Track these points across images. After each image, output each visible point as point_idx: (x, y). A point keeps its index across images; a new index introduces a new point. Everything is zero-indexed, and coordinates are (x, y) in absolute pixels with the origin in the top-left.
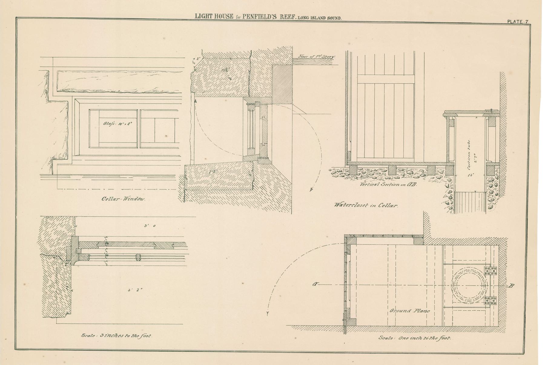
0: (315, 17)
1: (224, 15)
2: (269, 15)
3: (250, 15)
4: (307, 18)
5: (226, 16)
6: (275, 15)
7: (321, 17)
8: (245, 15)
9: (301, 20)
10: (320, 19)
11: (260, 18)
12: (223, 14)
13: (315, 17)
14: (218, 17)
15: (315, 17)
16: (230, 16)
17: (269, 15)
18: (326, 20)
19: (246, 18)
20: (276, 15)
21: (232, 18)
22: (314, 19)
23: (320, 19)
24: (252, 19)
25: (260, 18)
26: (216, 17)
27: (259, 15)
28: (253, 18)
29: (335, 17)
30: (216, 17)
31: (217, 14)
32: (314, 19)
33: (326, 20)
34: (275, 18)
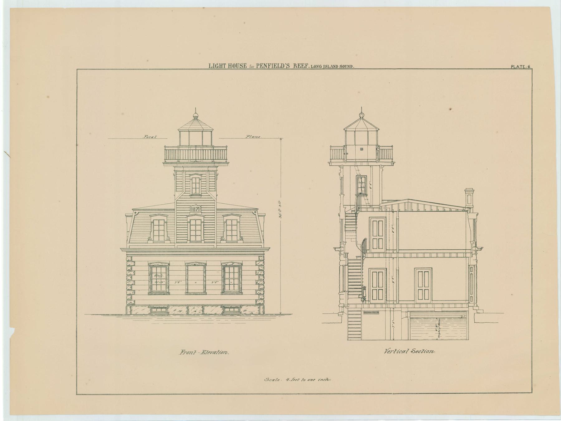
1: (238, 64)
2: (283, 65)
3: (264, 64)
5: (240, 66)
6: (288, 64)
7: (334, 66)
8: (258, 65)
9: (314, 68)
12: (237, 64)
16: (243, 66)
17: (283, 65)
18: (339, 68)
19: (259, 67)
21: (245, 67)
22: (326, 67)
25: (273, 67)
26: (230, 67)
28: (266, 66)
30: (230, 67)
31: (231, 64)
32: (326, 67)
33: (339, 68)
34: (288, 67)
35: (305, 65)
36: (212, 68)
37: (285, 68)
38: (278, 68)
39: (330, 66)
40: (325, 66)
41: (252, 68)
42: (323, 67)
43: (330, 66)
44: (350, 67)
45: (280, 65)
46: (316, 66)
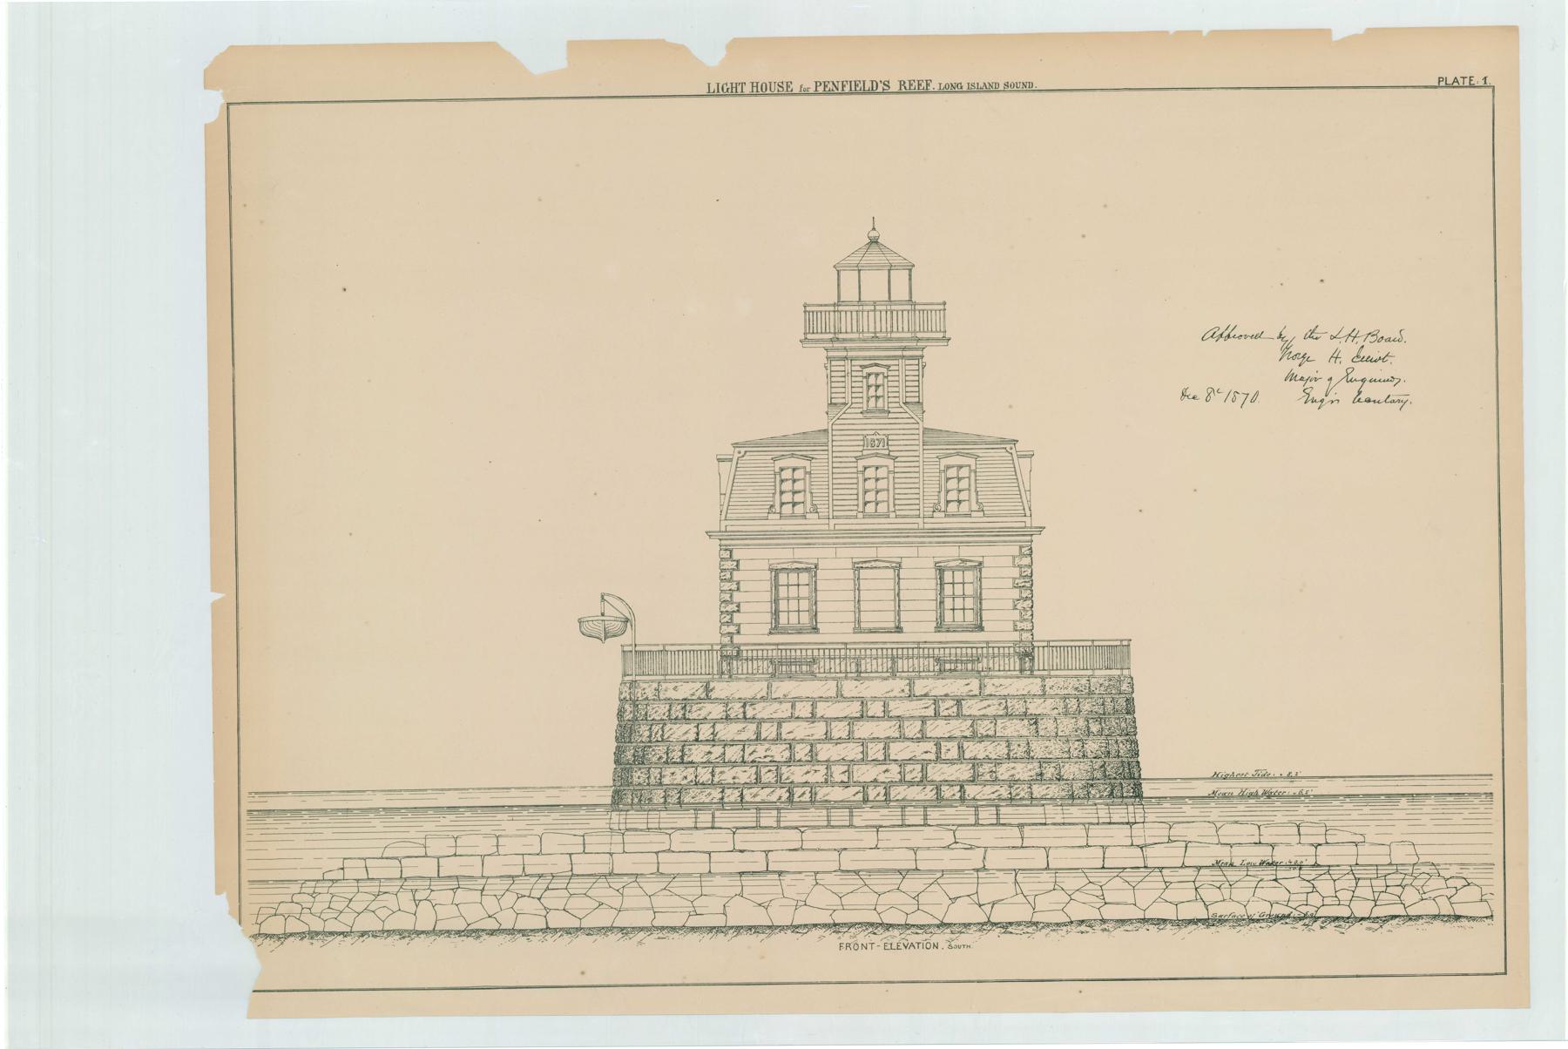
1: (773, 84)
2: (874, 83)
3: (831, 83)
5: (777, 86)
8: (818, 84)
11: (853, 89)
13: (976, 86)
14: (759, 88)
16: (785, 86)
17: (874, 83)
19: (821, 89)
20: (888, 82)
21: (789, 90)
24: (836, 91)
25: (853, 89)
26: (755, 89)
27: (851, 82)
30: (755, 89)
31: (757, 83)
34: (885, 87)
35: (924, 84)
37: (880, 90)
38: (864, 92)
39: (981, 85)
41: (804, 92)
42: (965, 88)
44: (1028, 87)
45: (868, 85)
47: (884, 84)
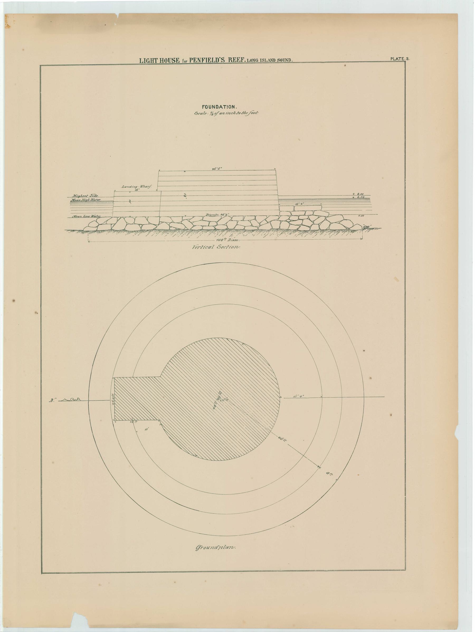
0: (265, 59)
4: (257, 61)
7: (271, 59)
10: (270, 61)
13: (264, 60)
15: (265, 59)
23: (270, 61)
28: (272, 61)
29: (285, 59)
33: (276, 61)
35: (240, 59)
36: (215, 62)
40: (262, 60)
43: (267, 60)
44: (288, 61)
46: (252, 60)
47: (172, 60)
